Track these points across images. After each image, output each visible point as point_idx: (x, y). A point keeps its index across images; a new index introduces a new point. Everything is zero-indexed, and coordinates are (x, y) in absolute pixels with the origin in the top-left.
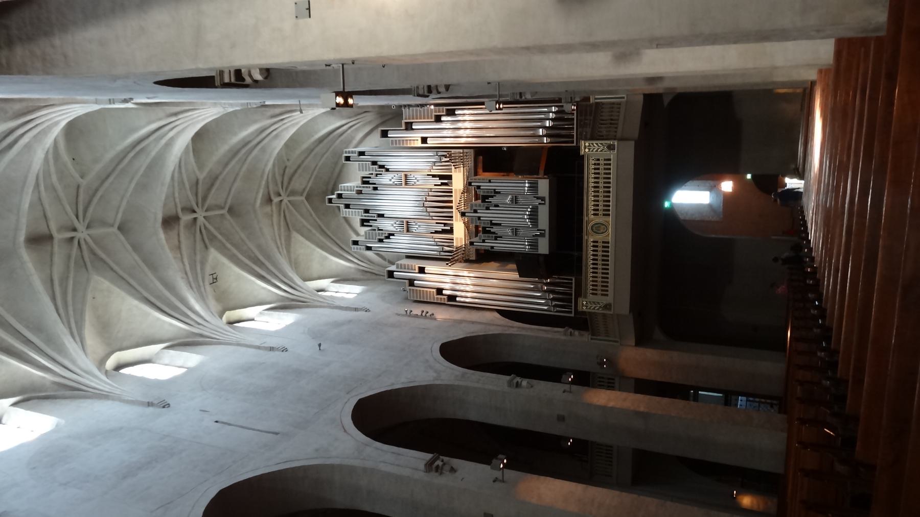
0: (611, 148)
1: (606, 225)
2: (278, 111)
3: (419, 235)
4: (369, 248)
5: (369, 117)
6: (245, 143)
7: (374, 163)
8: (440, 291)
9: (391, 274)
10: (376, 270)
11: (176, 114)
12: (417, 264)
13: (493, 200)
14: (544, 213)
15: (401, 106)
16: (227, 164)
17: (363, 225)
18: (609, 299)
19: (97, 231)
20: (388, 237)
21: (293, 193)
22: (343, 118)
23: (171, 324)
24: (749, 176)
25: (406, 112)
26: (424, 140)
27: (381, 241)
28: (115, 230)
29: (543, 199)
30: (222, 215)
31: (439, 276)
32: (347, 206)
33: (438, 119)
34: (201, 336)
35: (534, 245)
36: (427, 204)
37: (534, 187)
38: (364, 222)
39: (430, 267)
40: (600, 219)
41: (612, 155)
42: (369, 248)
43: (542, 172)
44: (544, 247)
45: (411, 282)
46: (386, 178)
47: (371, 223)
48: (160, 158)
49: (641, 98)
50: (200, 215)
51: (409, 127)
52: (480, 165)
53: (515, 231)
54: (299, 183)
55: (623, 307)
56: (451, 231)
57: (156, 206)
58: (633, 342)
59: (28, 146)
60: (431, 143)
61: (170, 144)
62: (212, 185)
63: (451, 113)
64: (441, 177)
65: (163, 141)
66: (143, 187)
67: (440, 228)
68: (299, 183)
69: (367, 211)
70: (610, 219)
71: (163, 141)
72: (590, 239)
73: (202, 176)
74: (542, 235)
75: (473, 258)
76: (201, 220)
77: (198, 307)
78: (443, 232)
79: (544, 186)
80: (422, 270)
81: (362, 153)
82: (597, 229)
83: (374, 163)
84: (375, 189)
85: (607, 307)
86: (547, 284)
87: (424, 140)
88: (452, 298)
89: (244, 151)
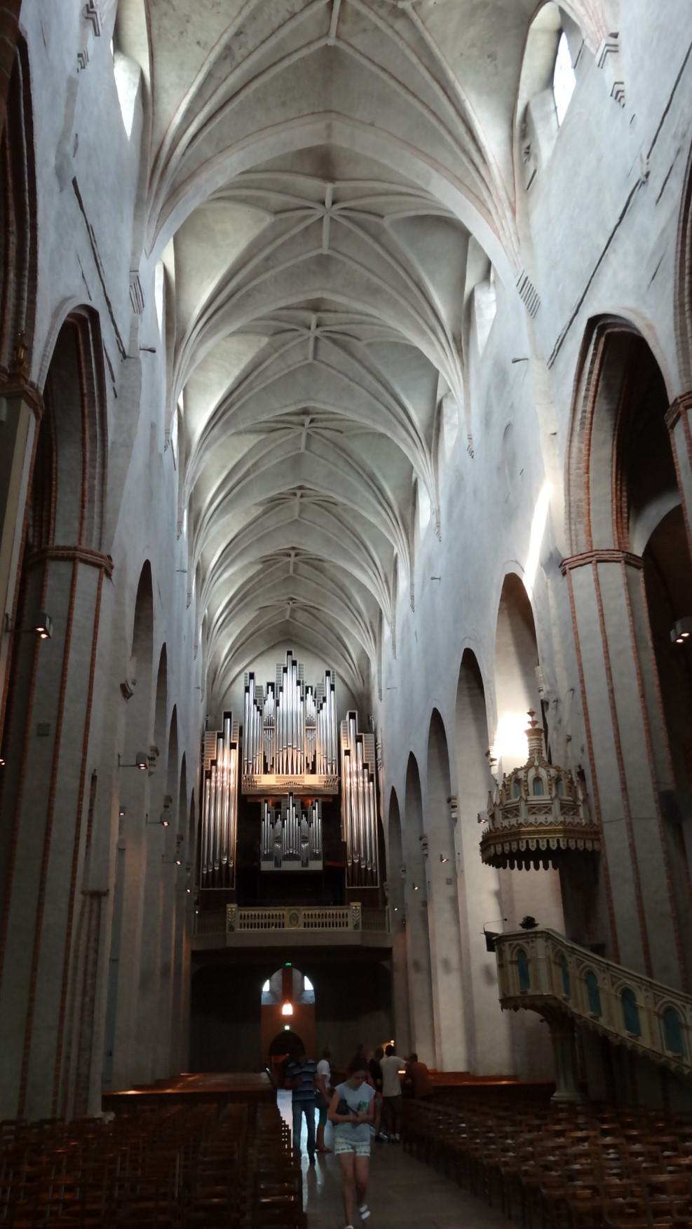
0: (356, 926)
1: (295, 924)
2: (376, 630)
5: (359, 684)
6: (349, 598)
7: (324, 699)
8: (214, 763)
9: (228, 715)
10: (217, 683)
11: (387, 582)
13: (304, 821)
14: (295, 866)
15: (375, 733)
16: (332, 580)
17: (269, 684)
19: (297, 510)
20: (258, 709)
21: (293, 611)
22: (359, 660)
24: (287, 1028)
25: (371, 736)
27: (255, 702)
28: (296, 517)
29: (306, 865)
30: (288, 572)
31: (228, 761)
33: (365, 766)
35: (268, 857)
36: (290, 749)
37: (316, 857)
38: (271, 684)
39: (235, 753)
40: (301, 920)
41: (350, 928)
43: (329, 863)
44: (267, 866)
45: (222, 736)
46: (311, 708)
47: (271, 693)
48: (351, 559)
49: (389, 945)
50: (292, 559)
51: (358, 739)
52: (325, 800)
53: (278, 839)
54: (302, 616)
55: (232, 942)
56: (266, 771)
57: (313, 547)
58: (195, 948)
59: (379, 513)
60: (344, 758)
61: (362, 568)
62: (316, 568)
63: (371, 779)
64: (314, 763)
65: (365, 565)
66: (328, 540)
67: (270, 764)
68: (301, 615)
69: (281, 689)
70: (302, 928)
71: (365, 565)
72: (285, 912)
73: (325, 565)
74: (278, 864)
76: (288, 559)
78: (266, 765)
79: (317, 865)
80: (233, 746)
84: (302, 699)
85: (232, 928)
87: (348, 753)
88: (209, 775)
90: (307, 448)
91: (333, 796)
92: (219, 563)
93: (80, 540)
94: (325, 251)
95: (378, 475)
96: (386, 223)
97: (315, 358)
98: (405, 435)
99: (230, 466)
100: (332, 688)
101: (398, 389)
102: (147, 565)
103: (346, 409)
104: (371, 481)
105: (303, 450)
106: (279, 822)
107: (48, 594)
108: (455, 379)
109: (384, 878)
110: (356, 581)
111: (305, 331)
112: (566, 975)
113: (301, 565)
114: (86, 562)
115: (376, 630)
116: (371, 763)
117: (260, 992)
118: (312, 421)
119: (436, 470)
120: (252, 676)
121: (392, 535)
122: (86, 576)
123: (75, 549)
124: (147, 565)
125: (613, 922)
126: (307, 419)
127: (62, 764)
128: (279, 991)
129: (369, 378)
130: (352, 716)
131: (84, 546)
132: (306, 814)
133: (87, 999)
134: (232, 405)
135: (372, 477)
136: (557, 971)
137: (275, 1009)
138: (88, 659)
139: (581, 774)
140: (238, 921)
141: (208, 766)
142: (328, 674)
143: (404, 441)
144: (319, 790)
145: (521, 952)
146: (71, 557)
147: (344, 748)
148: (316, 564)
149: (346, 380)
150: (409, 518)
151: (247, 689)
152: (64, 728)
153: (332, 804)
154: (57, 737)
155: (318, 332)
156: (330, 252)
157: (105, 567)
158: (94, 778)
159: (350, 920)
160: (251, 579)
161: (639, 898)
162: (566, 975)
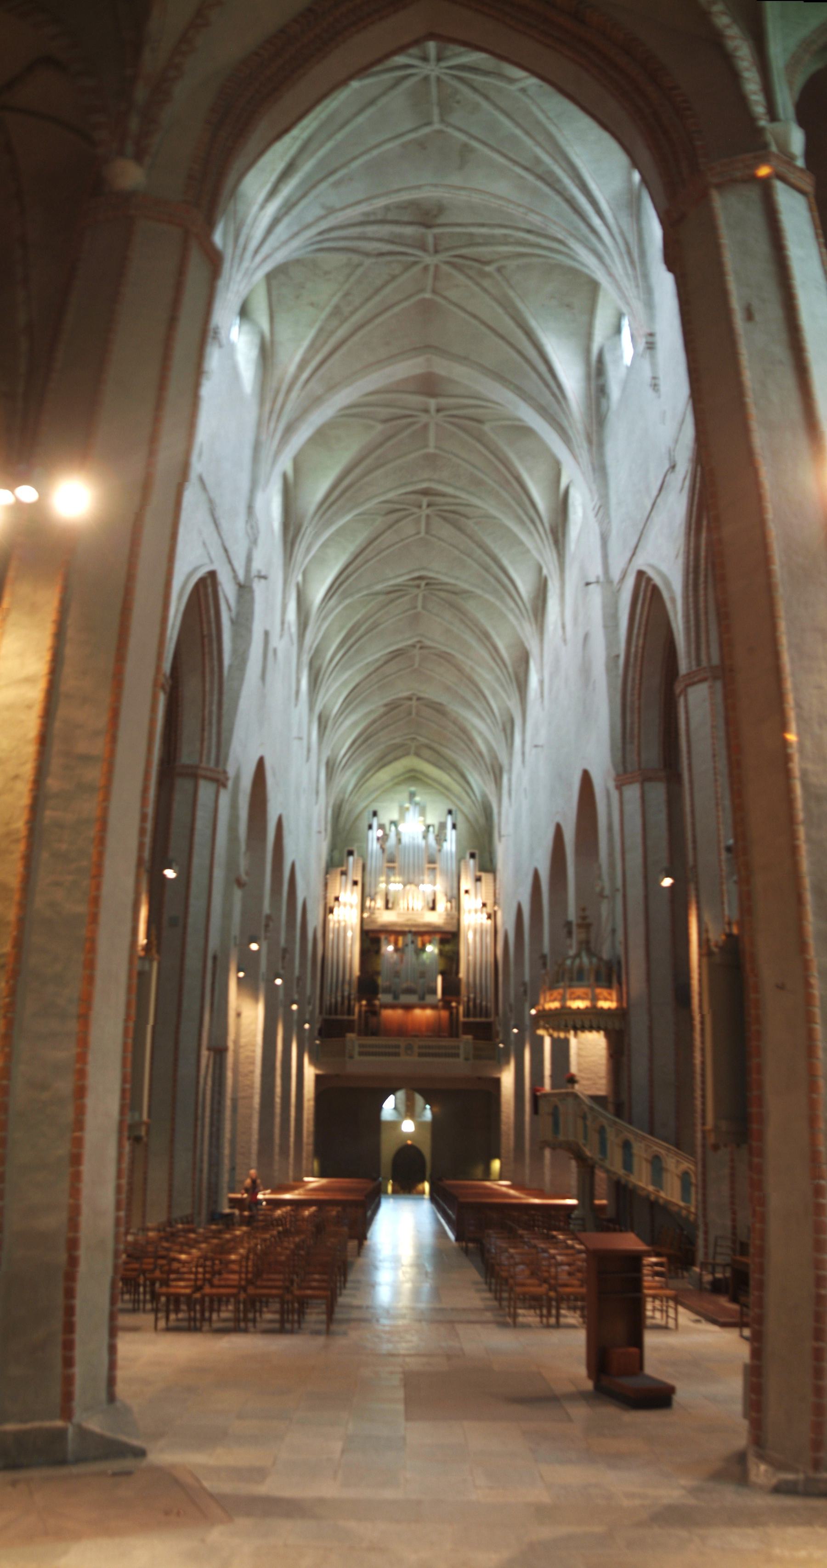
0: (467, 1059)
5: (482, 820)
9: (350, 853)
12: (359, 878)
18: (357, 1057)
19: (417, 659)
23: (335, 703)
33: (484, 905)
34: (325, 727)
35: (387, 990)
41: (461, 1059)
48: (469, 706)
50: (414, 703)
51: (478, 879)
56: (387, 908)
61: (480, 716)
64: (434, 902)
65: (483, 713)
66: (448, 689)
75: (366, 927)
76: (409, 703)
77: (348, 722)
78: (387, 902)
80: (355, 883)
82: (409, 1048)
85: (351, 1057)
86: (350, 995)
87: (467, 892)
89: (465, 738)
90: (424, 608)
92: (341, 712)
93: (201, 761)
94: (431, 450)
95: (493, 633)
96: (486, 428)
97: (427, 533)
98: (512, 605)
99: (349, 625)
100: (454, 826)
101: (506, 562)
102: (261, 763)
103: (457, 578)
104: (485, 637)
105: (419, 609)
107: (175, 806)
108: (551, 566)
109: (497, 1013)
110: (474, 727)
111: (415, 510)
112: (585, 1126)
114: (206, 778)
116: (490, 903)
117: (380, 1108)
118: (427, 584)
119: (542, 640)
120: (375, 814)
121: (505, 691)
122: (205, 790)
123: (197, 767)
124: (261, 763)
125: (630, 1087)
126: (423, 583)
127: (189, 949)
128: (402, 1108)
129: (479, 552)
130: (473, 856)
131: (204, 765)
133: (214, 1129)
134: (348, 577)
135: (487, 636)
136: (580, 1122)
137: (395, 1125)
138: (207, 862)
139: (619, 963)
140: (357, 1049)
141: (331, 902)
142: (450, 812)
143: (512, 610)
144: (438, 927)
145: (556, 1108)
146: (194, 774)
147: (463, 889)
148: (439, 709)
149: (457, 552)
150: (522, 675)
151: (370, 827)
152: (191, 920)
153: (449, 937)
154: (185, 927)
156: (437, 452)
157: (220, 782)
158: (215, 958)
159: (461, 1051)
160: (374, 722)
161: (651, 1070)
162: (585, 1126)
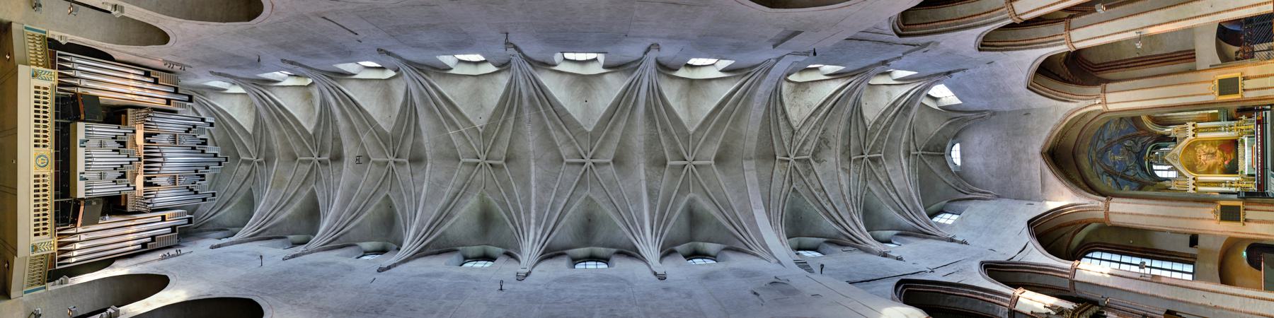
3: (167, 133)
4: (203, 120)
7: (196, 193)
8: (156, 82)
12: (171, 107)
13: (117, 174)
25: (175, 241)
26: (163, 218)
32: (216, 155)
39: (161, 104)
42: (203, 120)
45: (176, 92)
49: (13, 295)
51: (173, 228)
68: (245, 169)
80: (169, 102)
81: (204, 200)
83: (196, 193)
87: (163, 218)
88: (147, 75)
91: (125, 207)
94: (669, 163)
106: (117, 146)
113: (308, 167)
115: (261, 236)
116: (157, 244)
130: (190, 220)
132: (124, 176)
147: (167, 213)
155: (589, 163)
